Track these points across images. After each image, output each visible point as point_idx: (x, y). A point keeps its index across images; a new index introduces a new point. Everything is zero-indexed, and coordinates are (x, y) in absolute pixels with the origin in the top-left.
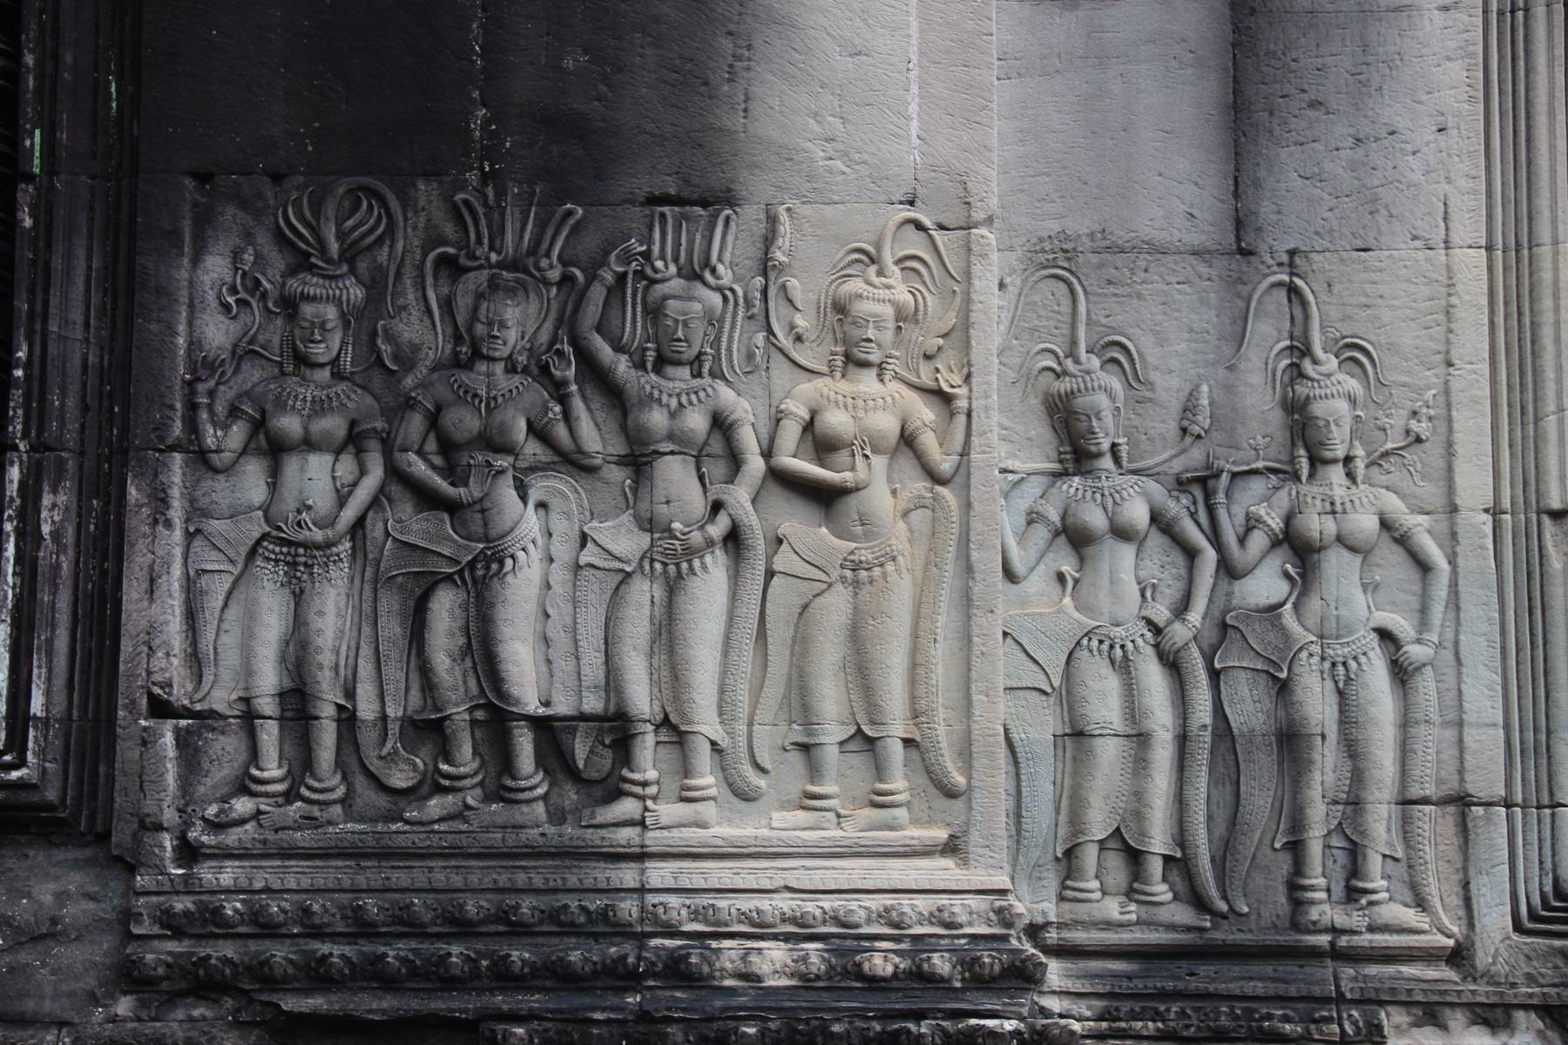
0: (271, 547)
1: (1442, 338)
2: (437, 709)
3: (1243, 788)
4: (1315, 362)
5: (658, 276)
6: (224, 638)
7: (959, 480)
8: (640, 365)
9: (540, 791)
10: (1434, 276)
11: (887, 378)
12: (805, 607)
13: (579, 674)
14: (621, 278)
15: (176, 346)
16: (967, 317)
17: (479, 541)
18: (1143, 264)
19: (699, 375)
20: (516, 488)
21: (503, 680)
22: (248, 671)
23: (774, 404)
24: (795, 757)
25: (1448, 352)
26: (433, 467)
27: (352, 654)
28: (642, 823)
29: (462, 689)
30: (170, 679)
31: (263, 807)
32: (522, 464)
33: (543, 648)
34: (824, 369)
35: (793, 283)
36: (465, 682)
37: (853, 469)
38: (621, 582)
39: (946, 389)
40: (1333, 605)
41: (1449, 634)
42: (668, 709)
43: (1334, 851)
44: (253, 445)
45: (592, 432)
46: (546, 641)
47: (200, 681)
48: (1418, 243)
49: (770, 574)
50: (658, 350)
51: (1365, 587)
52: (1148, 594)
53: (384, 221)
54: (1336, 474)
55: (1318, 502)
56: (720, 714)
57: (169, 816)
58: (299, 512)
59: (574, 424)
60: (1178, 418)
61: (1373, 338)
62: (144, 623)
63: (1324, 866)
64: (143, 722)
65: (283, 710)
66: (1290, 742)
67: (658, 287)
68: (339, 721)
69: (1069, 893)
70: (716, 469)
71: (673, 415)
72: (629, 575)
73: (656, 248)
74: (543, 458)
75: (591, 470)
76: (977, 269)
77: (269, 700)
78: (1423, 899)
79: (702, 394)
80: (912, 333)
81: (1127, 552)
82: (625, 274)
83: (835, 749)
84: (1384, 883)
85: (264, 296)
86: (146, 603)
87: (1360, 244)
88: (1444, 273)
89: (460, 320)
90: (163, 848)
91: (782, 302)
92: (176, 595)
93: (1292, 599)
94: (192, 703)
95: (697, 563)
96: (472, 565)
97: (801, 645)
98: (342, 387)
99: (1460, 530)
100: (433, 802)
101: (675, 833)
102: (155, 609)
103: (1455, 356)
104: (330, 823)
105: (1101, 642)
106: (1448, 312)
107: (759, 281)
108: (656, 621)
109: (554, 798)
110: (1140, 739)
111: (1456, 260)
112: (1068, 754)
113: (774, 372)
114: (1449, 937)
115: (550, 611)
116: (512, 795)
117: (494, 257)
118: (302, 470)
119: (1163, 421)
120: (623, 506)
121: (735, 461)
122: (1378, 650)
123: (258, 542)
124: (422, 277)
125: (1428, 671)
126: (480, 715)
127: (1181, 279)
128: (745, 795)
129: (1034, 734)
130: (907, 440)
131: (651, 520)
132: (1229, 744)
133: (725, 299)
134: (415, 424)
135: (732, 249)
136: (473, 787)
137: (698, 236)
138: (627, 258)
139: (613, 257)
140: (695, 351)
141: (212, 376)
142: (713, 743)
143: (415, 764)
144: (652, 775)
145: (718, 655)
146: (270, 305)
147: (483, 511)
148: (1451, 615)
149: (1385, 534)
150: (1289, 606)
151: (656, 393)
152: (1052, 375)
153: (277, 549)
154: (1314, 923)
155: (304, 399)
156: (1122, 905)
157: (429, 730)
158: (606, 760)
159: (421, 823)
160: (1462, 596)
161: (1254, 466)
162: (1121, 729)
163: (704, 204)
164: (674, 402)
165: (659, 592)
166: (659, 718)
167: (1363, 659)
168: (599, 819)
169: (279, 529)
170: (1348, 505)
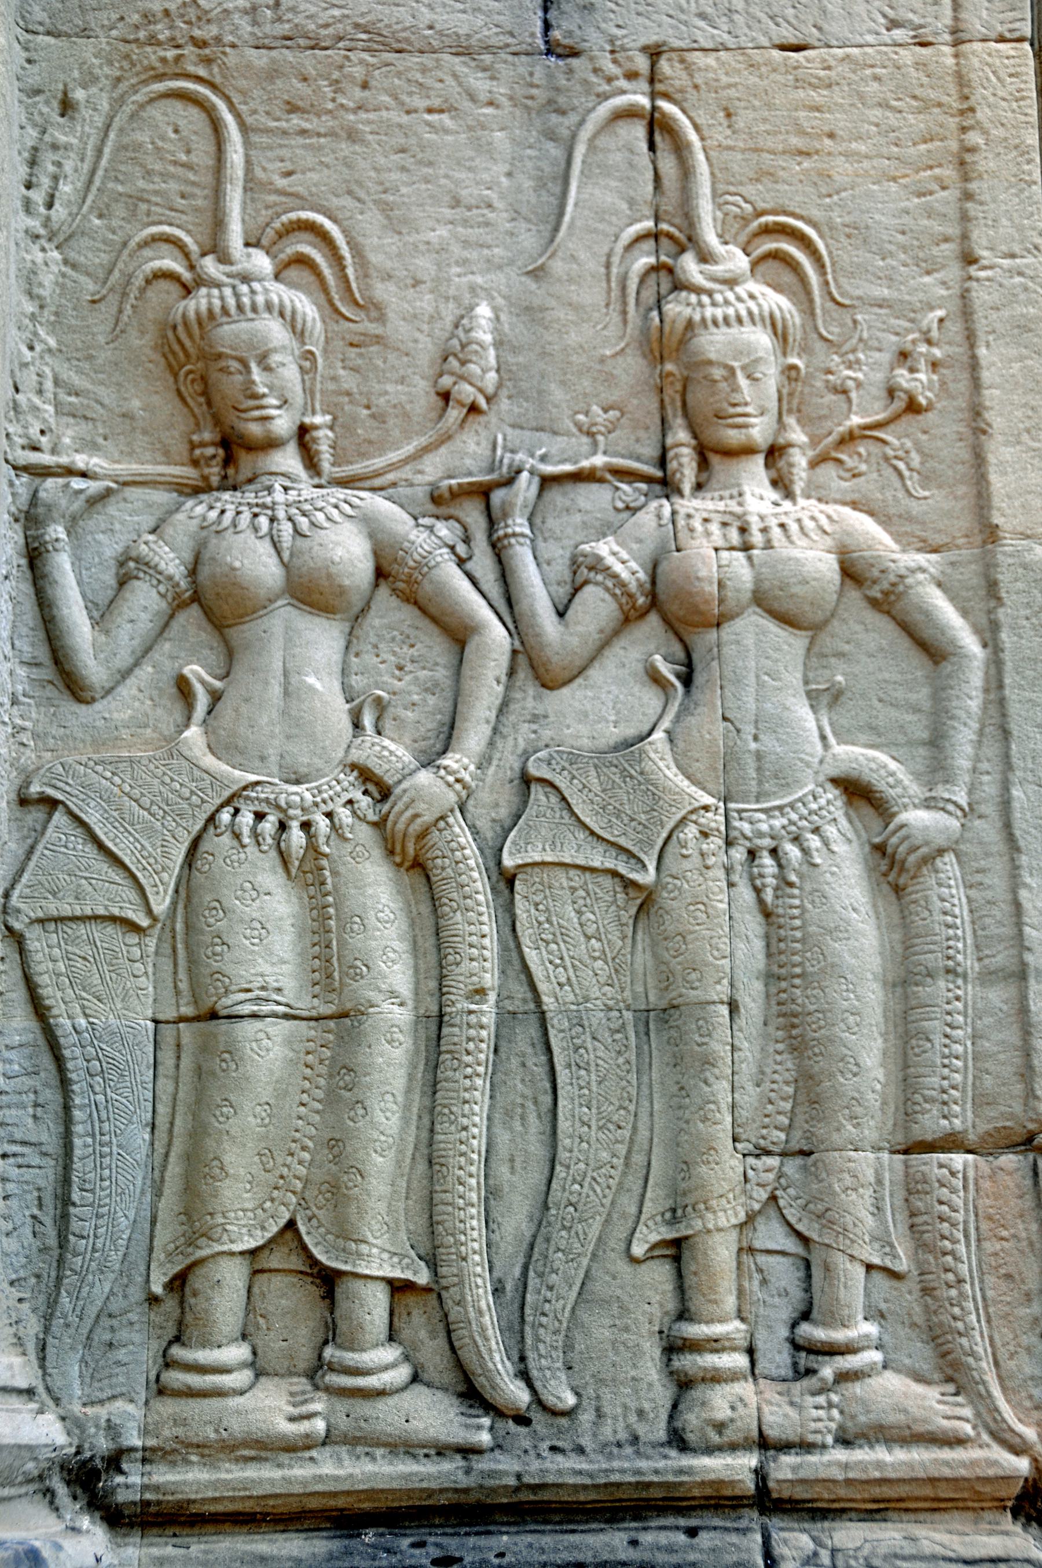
1: (952, 212)
3: (563, 1125)
4: (705, 257)
10: (932, 95)
18: (358, 72)
25: (965, 237)
40: (749, 730)
41: (989, 787)
43: (762, 1259)
48: (898, 34)
51: (813, 697)
52: (368, 721)
54: (754, 476)
55: (714, 528)
60: (430, 372)
61: (816, 214)
63: (741, 1293)
66: (663, 1020)
69: (176, 1378)
78: (956, 1365)
81: (321, 641)
84: (870, 1329)
87: (790, 36)
88: (953, 89)
93: (666, 723)
99: (1004, 577)
103: (980, 240)
105: (260, 816)
106: (964, 162)
110: (340, 1020)
111: (975, 62)
112: (186, 1062)
114: (1017, 1452)
119: (402, 380)
122: (843, 822)
125: (949, 864)
127: (436, 103)
129: (107, 1018)
132: (534, 1032)
148: (991, 750)
149: (854, 595)
150: (659, 735)
152: (175, 289)
154: (720, 1427)
156: (296, 1399)
160: (1014, 709)
161: (585, 464)
162: (305, 1004)
167: (814, 842)
170: (776, 532)
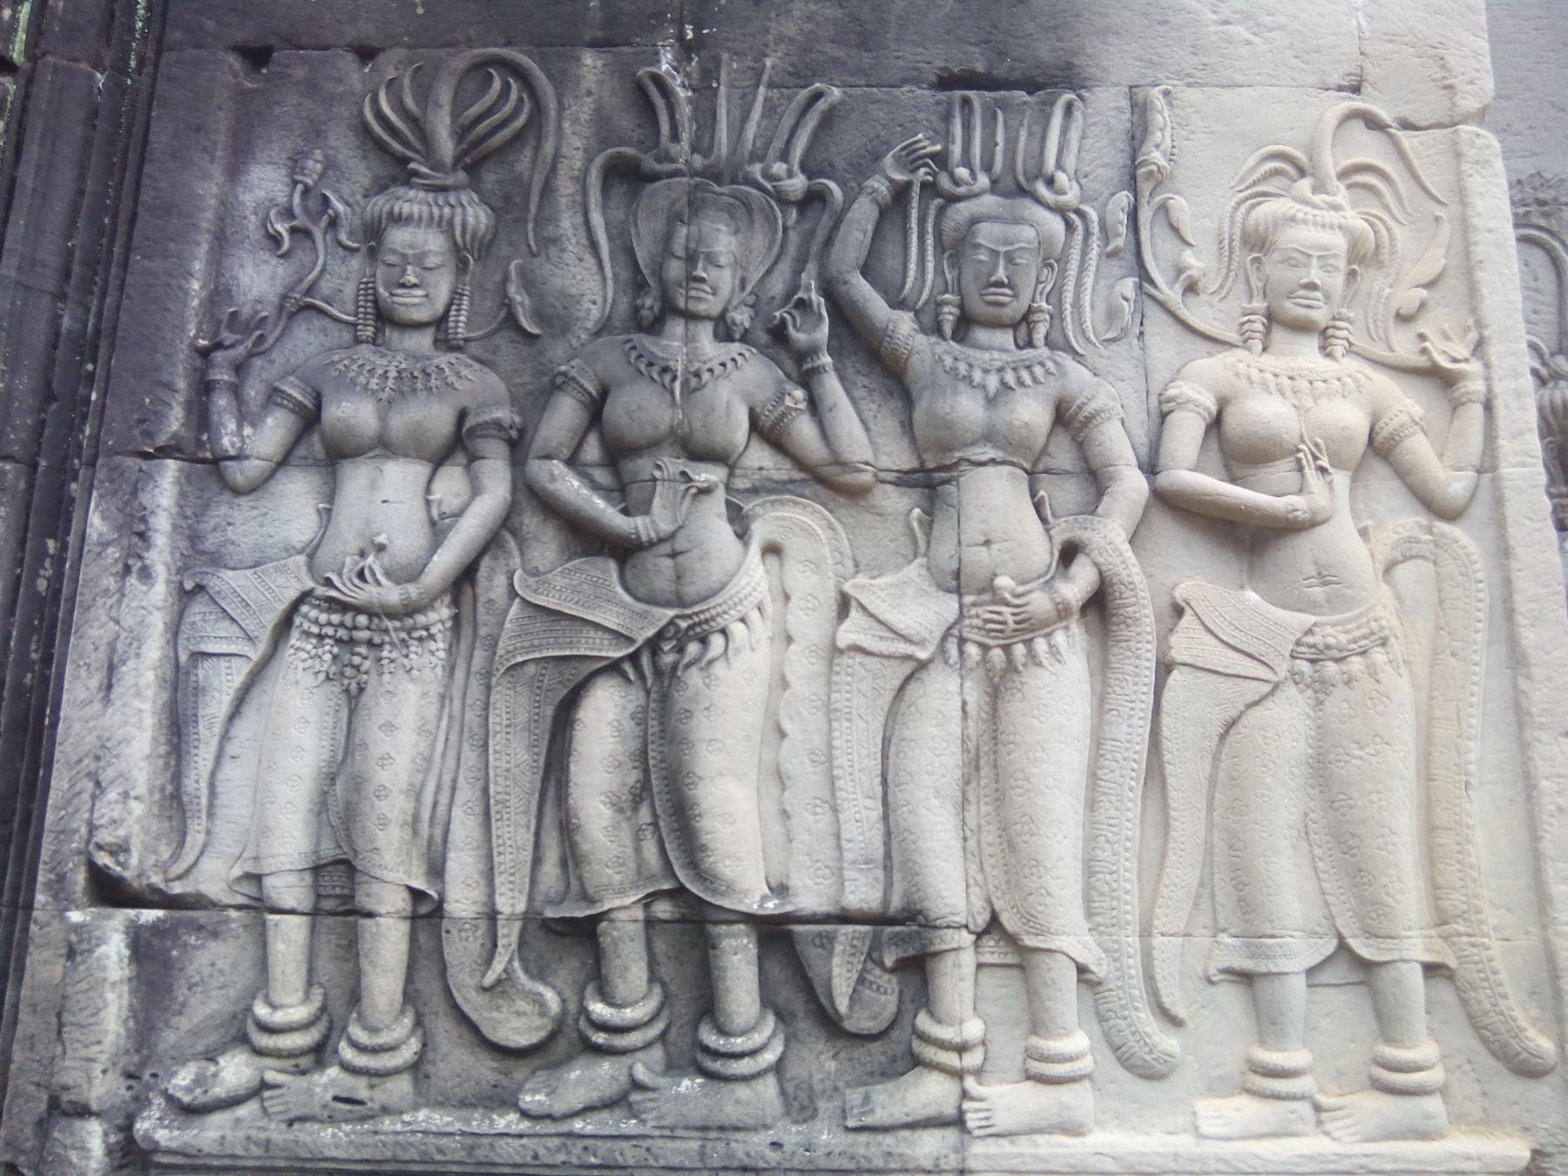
0: (313, 613)
2: (586, 898)
5: (962, 190)
6: (229, 771)
7: (1480, 511)
8: (935, 329)
9: (770, 1057)
11: (1338, 350)
12: (1231, 725)
13: (838, 837)
14: (901, 194)
15: (187, 293)
16: (1467, 254)
17: (667, 604)
19: (1030, 344)
20: (731, 520)
21: (704, 848)
22: (261, 830)
23: (1155, 388)
24: (1230, 997)
26: (596, 487)
27: (444, 799)
28: (958, 1122)
29: (632, 865)
30: (127, 839)
31: (271, 1076)
32: (741, 483)
33: (775, 791)
34: (1233, 337)
35: (1178, 204)
36: (638, 850)
37: (1301, 491)
38: (909, 678)
39: (1445, 363)
42: (999, 905)
44: (301, 451)
45: (859, 431)
46: (781, 778)
47: (182, 843)
49: (1165, 668)
50: (961, 306)
53: (526, 109)
56: (1090, 914)
57: (102, 1087)
58: (363, 554)
59: (828, 417)
62: (91, 739)
64: (75, 916)
65: (319, 896)
67: (961, 206)
68: (414, 918)
70: (1064, 493)
71: (991, 401)
72: (923, 665)
73: (956, 150)
74: (775, 475)
75: (855, 494)
76: (1475, 182)
77: (292, 879)
79: (1038, 370)
80: (1373, 281)
82: (908, 185)
83: (1300, 982)
85: (334, 223)
86: (97, 706)
89: (641, 255)
90: (84, 1149)
91: (1162, 232)
92: (150, 693)
94: (167, 881)
95: (1041, 645)
96: (654, 645)
97: (1228, 788)
98: (443, 359)
100: (575, 1074)
101: (1023, 1146)
102: (112, 717)
104: (385, 1110)
107: (1124, 198)
108: (972, 746)
109: (794, 1070)
113: (1152, 340)
115: (787, 726)
116: (717, 1066)
117: (698, 161)
118: (373, 486)
120: (909, 551)
121: (1096, 480)
123: (294, 607)
124: (584, 192)
126: (663, 909)
128: (1150, 1072)
130: (1381, 448)
131: (957, 575)
133: (1069, 226)
134: (564, 415)
135: (1078, 147)
136: (647, 1046)
137: (1023, 133)
138: (911, 160)
139: (888, 160)
140: (1021, 305)
141: (242, 342)
142: (1082, 970)
143: (540, 1002)
144: (973, 1029)
145: (1080, 806)
146: (343, 237)
147: (674, 555)
151: (963, 368)
153: (323, 618)
155: (385, 376)
157: (573, 937)
158: (886, 997)
159: (550, 1117)
163: (1032, 86)
164: (993, 382)
165: (975, 695)
166: (982, 919)
168: (880, 1117)
169: (328, 583)
